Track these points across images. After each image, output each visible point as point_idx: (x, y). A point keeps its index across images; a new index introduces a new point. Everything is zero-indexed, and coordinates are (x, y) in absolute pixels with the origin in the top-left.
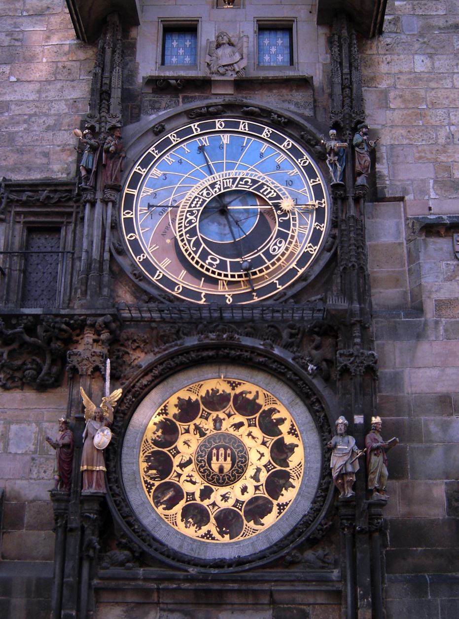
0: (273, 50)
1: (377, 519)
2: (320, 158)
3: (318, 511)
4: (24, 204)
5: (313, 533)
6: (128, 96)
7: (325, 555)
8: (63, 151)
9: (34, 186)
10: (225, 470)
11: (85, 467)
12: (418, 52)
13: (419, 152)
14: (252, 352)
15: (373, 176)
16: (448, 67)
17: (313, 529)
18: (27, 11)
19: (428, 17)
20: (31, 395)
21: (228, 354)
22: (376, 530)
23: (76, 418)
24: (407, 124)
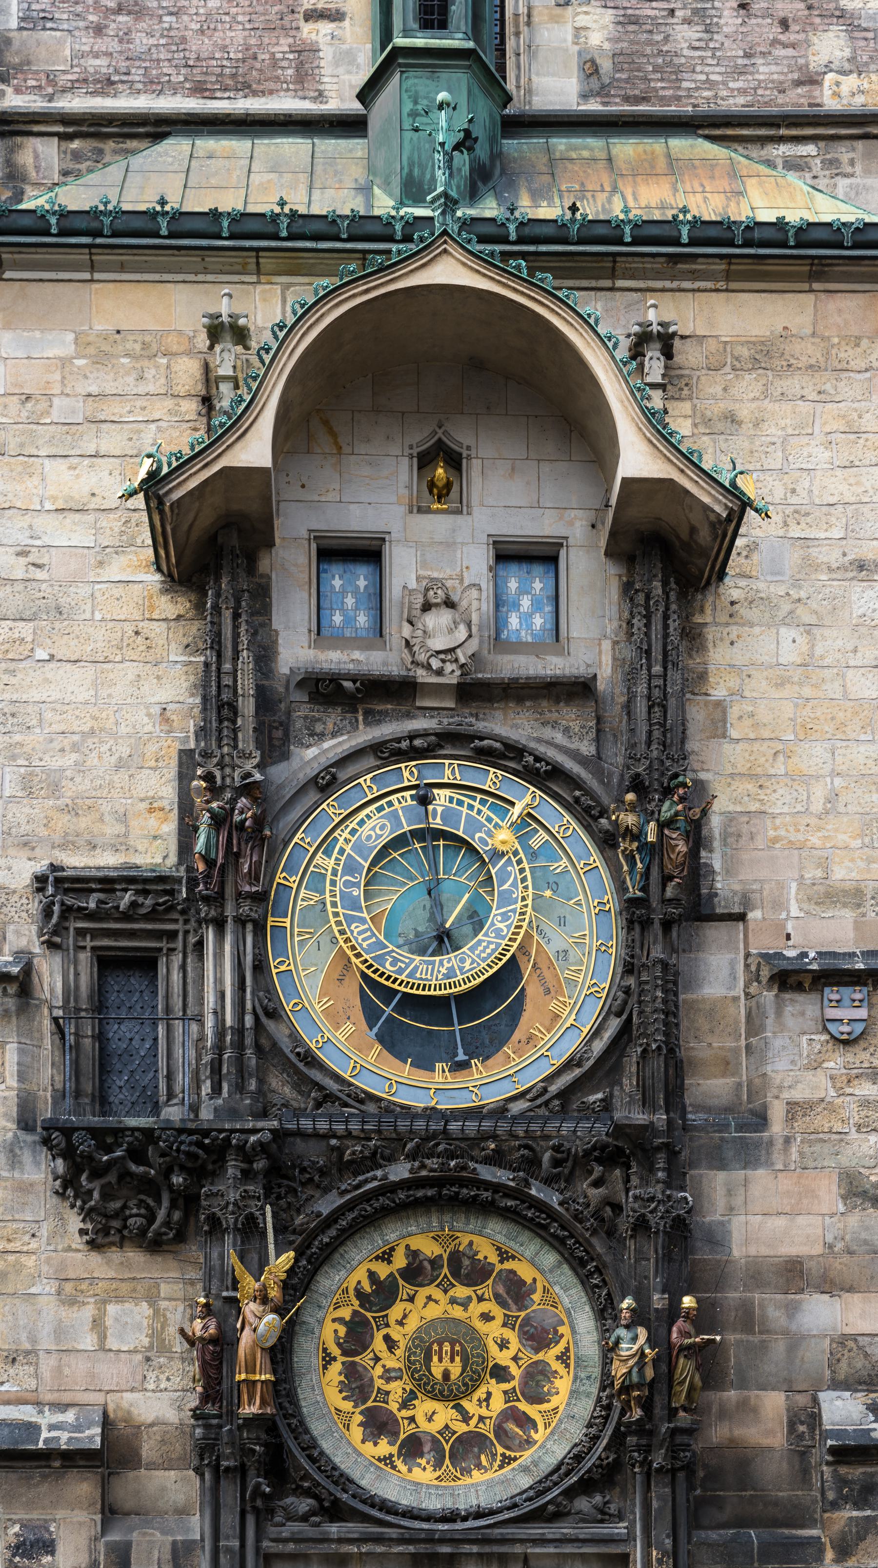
0: (526, 603)
1: (684, 1451)
2: (607, 842)
3: (595, 1439)
4: (92, 916)
5: (589, 1471)
6: (265, 701)
7: (606, 1503)
8: (151, 811)
9: (108, 883)
10: (453, 1377)
11: (243, 1376)
12: (787, 621)
13: (776, 829)
14: (495, 1192)
15: (696, 872)
16: (838, 656)
17: (589, 1464)
18: (54, 499)
19: (810, 543)
20: (135, 1256)
21: (457, 1194)
22: (682, 1468)
23: (225, 1298)
24: (759, 771)
